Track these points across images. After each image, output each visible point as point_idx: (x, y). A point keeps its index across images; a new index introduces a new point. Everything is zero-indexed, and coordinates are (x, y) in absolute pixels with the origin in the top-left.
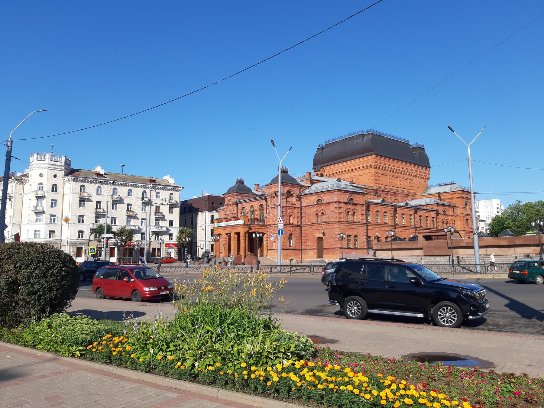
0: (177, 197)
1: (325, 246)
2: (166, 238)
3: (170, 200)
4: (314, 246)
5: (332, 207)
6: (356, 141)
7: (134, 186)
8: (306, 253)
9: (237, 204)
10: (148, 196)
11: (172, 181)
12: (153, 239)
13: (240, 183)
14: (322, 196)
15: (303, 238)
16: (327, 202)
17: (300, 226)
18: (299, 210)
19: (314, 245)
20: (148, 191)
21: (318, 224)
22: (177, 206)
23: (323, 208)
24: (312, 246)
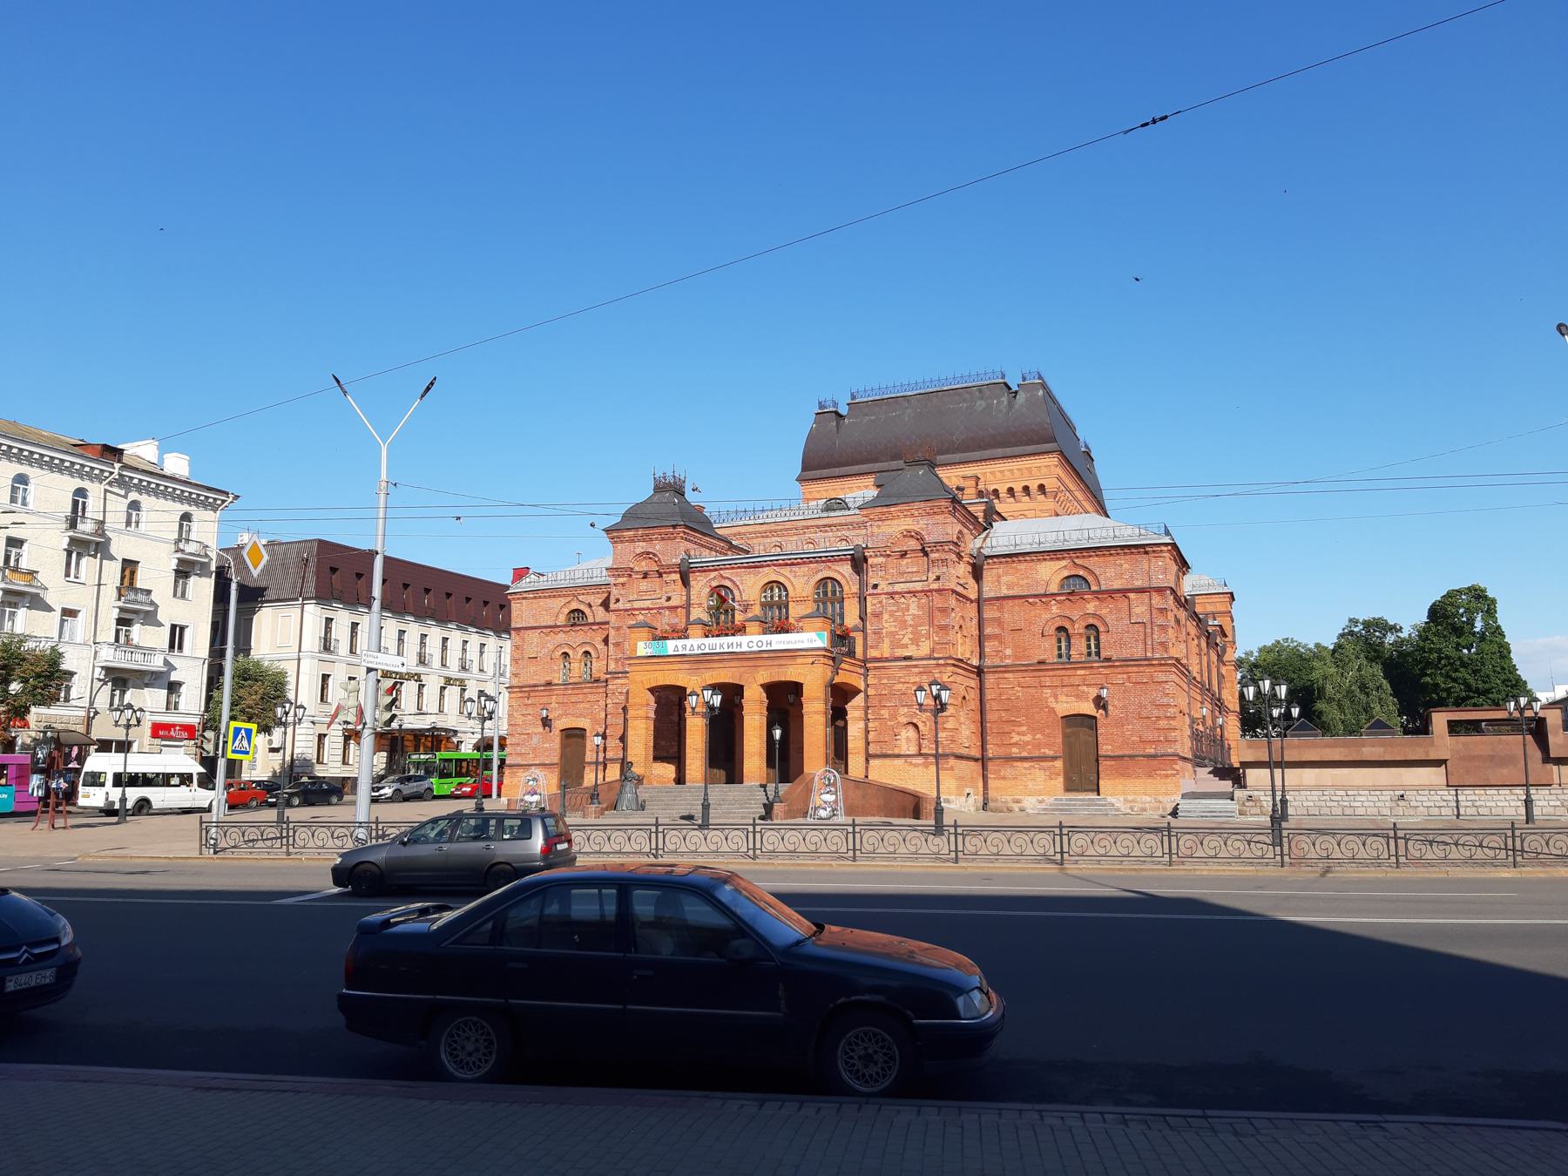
0: (208, 532)
1: (1105, 749)
2: (151, 700)
3: (179, 540)
4: (1049, 746)
6: (981, 404)
7: (41, 463)
8: (1007, 771)
9: (685, 574)
10: (93, 506)
11: (177, 465)
12: (102, 700)
13: (671, 488)
14: (1092, 562)
15: (990, 717)
16: (1117, 585)
17: (980, 672)
18: (972, 611)
19: (1053, 742)
20: (95, 490)
22: (203, 569)
23: (1091, 607)
24: (1038, 746)
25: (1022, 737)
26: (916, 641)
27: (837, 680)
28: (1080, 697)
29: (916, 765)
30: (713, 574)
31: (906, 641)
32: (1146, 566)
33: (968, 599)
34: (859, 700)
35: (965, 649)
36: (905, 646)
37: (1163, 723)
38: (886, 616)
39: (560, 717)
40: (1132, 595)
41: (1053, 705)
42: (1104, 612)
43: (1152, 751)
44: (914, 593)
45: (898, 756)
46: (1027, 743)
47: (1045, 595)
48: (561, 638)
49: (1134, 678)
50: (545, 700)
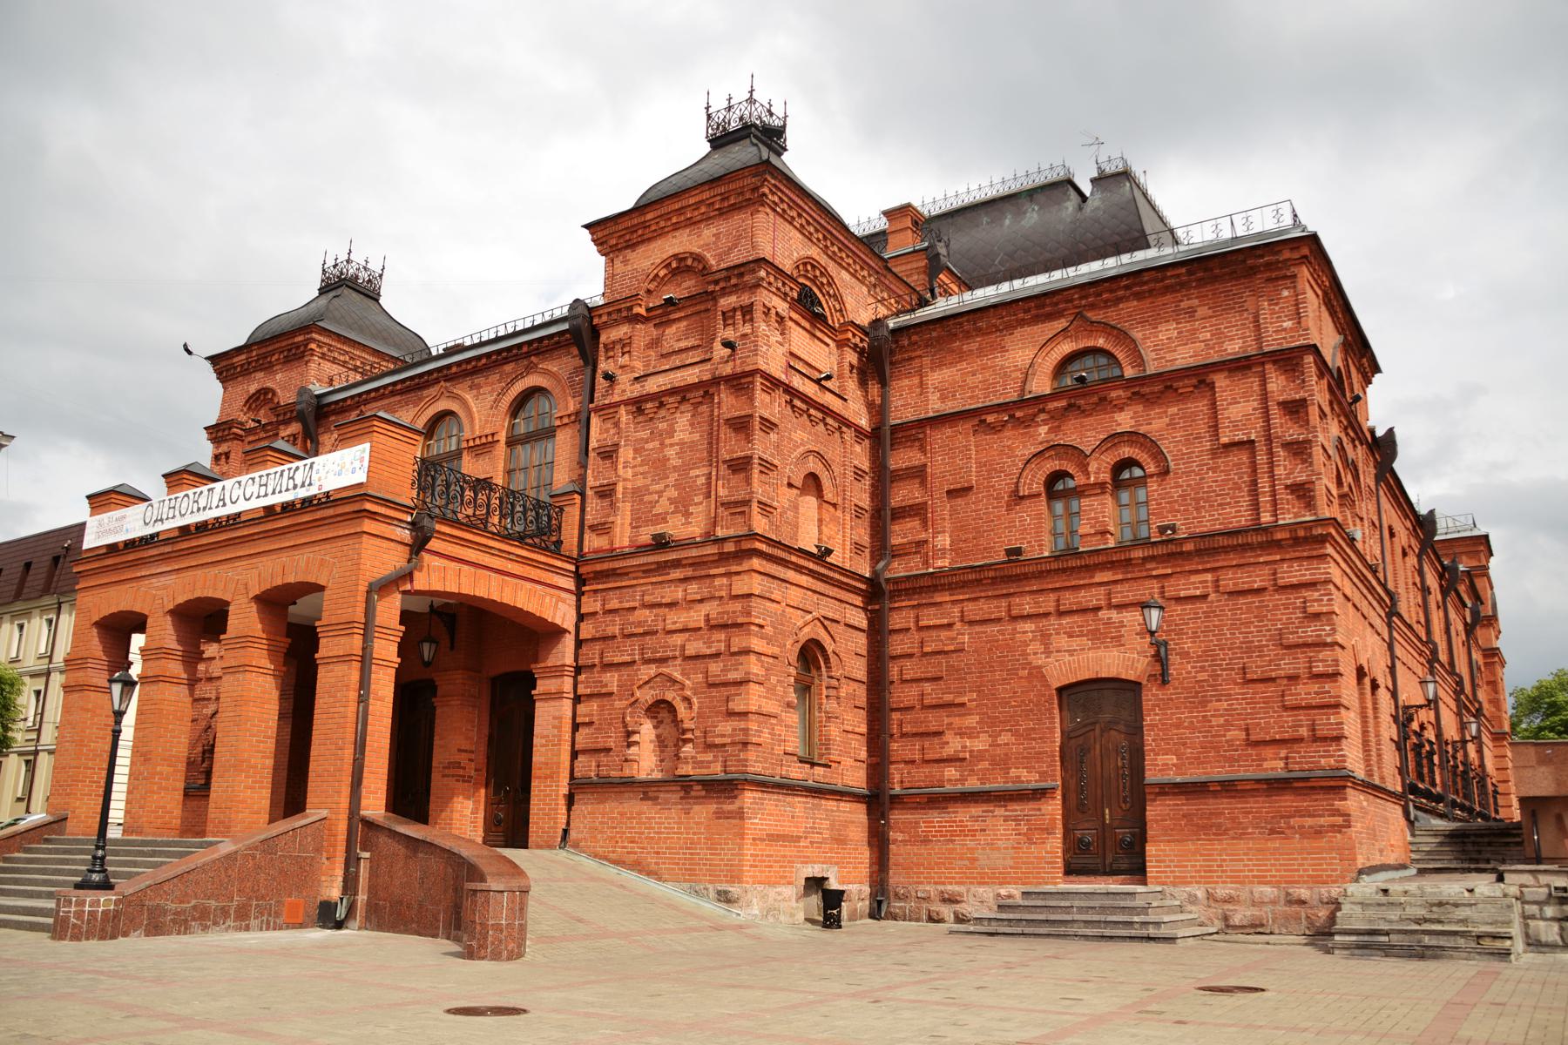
1: (1161, 766)
4: (1027, 760)
5: (1239, 408)
16: (1184, 357)
18: (860, 455)
21: (1071, 564)
24: (1003, 763)
26: (682, 506)
27: (421, 582)
28: (1099, 637)
31: (663, 506)
33: (844, 422)
34: (565, 652)
35: (829, 527)
37: (1306, 692)
38: (625, 454)
40: (1221, 381)
41: (1040, 660)
43: (1274, 766)
44: (682, 393)
46: (978, 756)
47: (1022, 403)
49: (1230, 580)
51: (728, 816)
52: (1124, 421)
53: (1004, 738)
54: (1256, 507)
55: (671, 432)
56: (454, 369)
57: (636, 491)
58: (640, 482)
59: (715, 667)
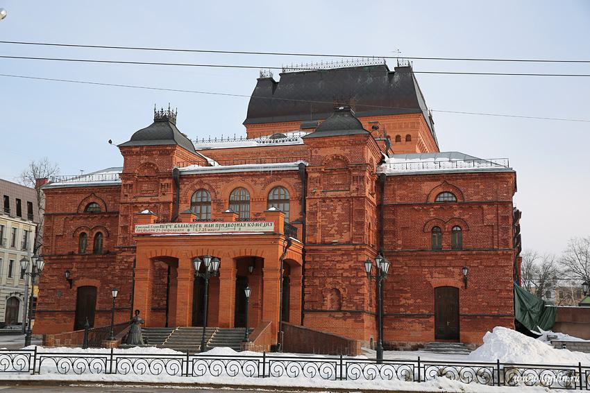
1: (464, 310)
8: (397, 324)
16: (475, 198)
24: (419, 307)
25: (407, 300)
26: (340, 232)
29: (337, 318)
30: (196, 180)
31: (333, 232)
32: (495, 187)
36: (333, 235)
38: (319, 214)
39: (78, 278)
40: (485, 207)
41: (430, 280)
42: (466, 217)
44: (340, 199)
45: (326, 311)
46: (411, 305)
47: (426, 204)
48: (80, 222)
50: (68, 266)
51: (360, 321)
52: (457, 214)
53: (419, 300)
54: (493, 244)
55: (335, 210)
56: (245, 174)
57: (322, 226)
58: (324, 223)
59: (353, 281)
